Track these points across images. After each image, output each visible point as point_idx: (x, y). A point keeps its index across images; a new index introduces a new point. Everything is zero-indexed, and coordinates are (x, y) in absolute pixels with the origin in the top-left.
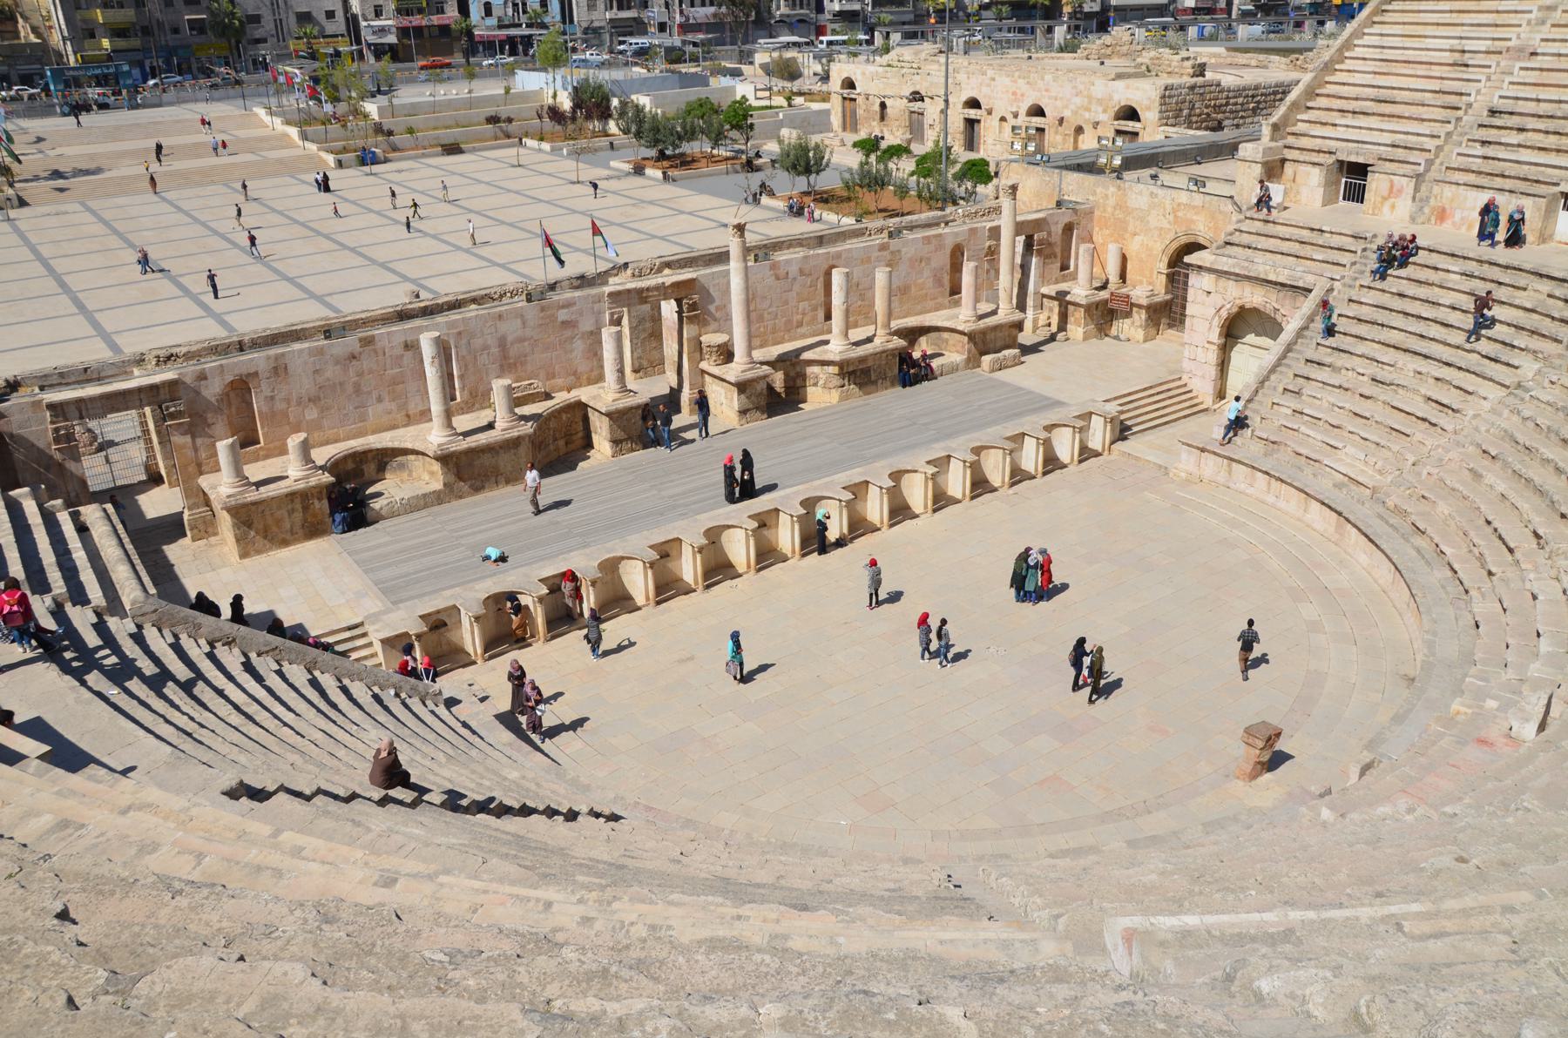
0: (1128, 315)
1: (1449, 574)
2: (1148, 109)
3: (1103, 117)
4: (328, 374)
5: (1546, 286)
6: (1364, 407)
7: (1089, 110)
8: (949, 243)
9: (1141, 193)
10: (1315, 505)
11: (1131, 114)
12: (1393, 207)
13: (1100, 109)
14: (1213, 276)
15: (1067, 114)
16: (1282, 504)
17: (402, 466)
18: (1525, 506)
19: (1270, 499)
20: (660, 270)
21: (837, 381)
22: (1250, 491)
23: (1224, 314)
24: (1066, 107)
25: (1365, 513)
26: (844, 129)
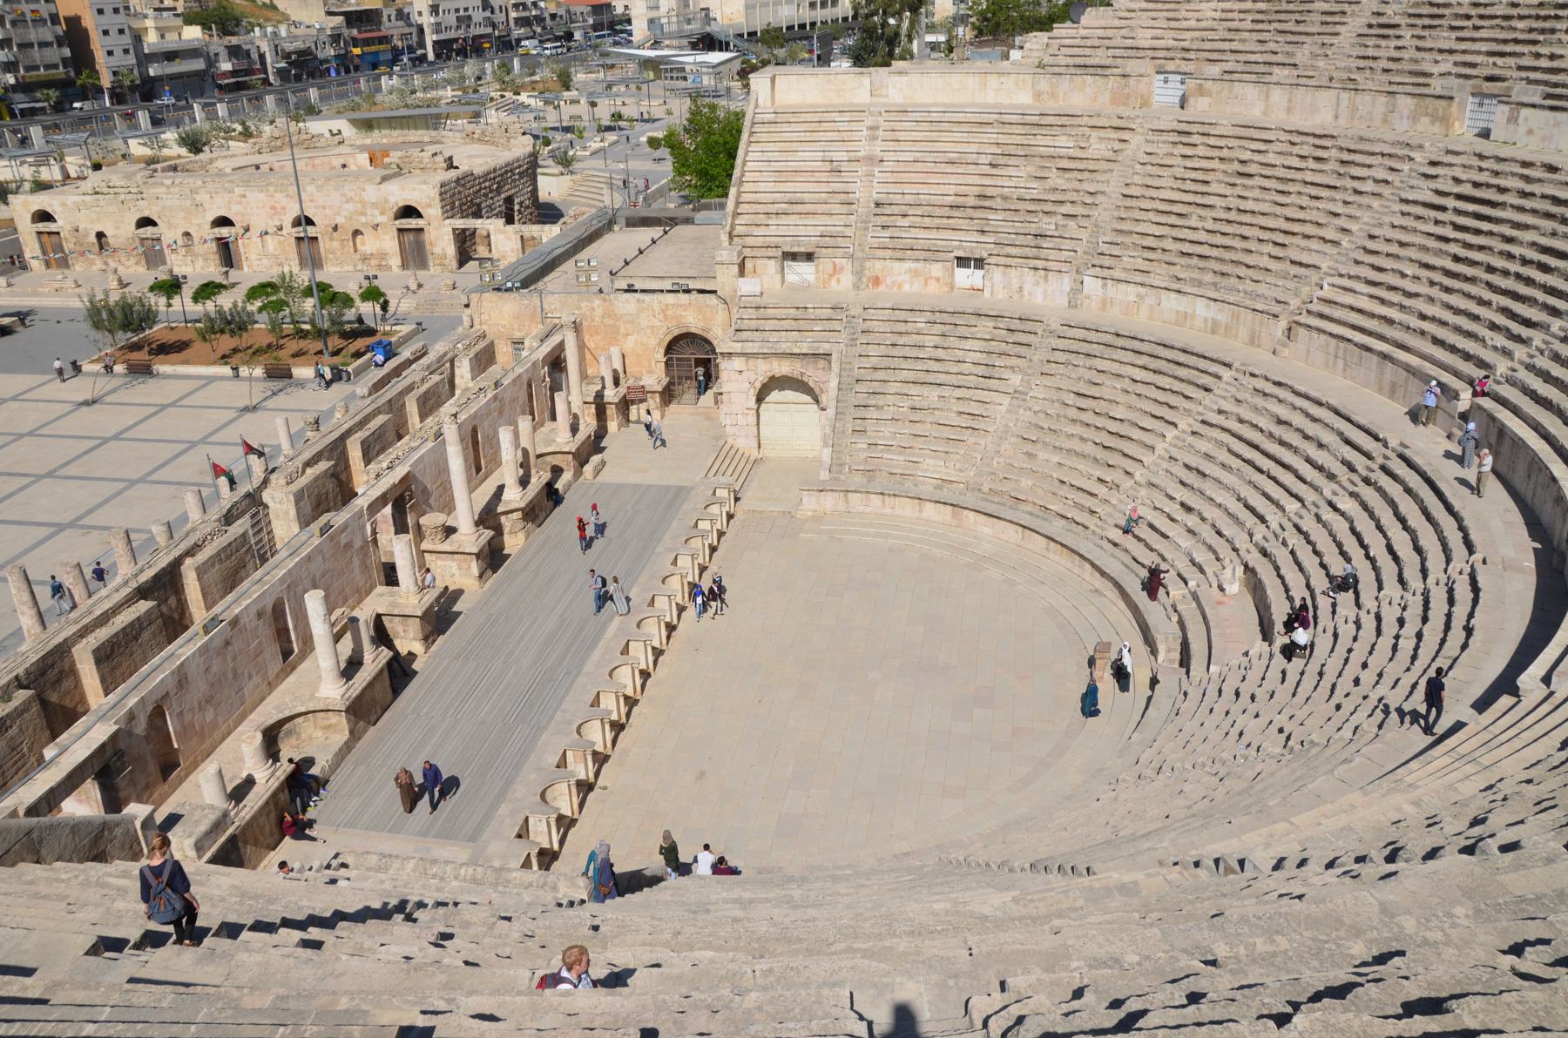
1: (1064, 522)
2: (429, 206)
3: (380, 219)
4: (214, 669)
5: (990, 323)
6: (918, 429)
10: (929, 506)
11: (409, 212)
13: (377, 212)
15: (340, 220)
16: (898, 512)
17: (289, 733)
18: (1081, 467)
19: (888, 511)
20: (303, 472)
21: (521, 524)
22: (868, 510)
23: (758, 385)
25: (969, 500)
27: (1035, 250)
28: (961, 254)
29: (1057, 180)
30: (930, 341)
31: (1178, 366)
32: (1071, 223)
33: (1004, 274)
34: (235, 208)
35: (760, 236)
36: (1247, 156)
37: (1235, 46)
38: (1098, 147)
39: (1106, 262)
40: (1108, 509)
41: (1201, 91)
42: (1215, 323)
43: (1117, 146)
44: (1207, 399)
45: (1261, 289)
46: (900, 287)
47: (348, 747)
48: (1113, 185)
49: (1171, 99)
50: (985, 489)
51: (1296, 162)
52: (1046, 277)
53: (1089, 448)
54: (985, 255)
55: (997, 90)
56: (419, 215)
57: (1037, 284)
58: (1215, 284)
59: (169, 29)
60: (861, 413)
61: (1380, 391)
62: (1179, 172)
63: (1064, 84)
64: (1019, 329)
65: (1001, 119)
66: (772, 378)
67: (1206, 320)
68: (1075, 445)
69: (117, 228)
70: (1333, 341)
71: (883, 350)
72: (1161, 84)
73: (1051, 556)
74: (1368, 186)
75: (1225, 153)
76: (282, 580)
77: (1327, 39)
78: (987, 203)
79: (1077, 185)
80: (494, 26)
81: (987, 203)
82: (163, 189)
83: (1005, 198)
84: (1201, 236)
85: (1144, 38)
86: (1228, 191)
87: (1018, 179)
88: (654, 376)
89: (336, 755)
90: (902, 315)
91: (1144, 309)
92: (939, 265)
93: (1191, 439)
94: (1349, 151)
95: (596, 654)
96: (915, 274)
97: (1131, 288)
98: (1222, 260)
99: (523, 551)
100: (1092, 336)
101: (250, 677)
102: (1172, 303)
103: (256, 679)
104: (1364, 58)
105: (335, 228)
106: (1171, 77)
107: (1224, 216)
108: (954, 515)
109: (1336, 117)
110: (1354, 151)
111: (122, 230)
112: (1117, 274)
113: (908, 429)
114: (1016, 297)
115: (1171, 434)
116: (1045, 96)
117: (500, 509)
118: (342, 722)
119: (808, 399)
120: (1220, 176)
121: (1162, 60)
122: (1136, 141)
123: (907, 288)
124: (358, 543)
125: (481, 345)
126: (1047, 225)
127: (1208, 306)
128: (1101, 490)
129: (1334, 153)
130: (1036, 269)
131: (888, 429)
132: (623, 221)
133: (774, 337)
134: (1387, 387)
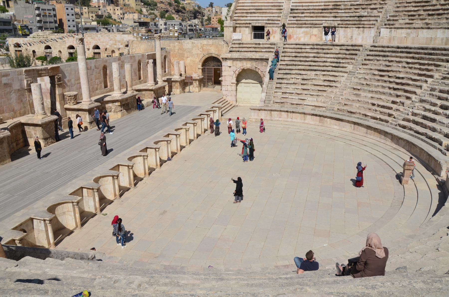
0: (191, 84)
3: (121, 46)
5: (338, 48)
6: (305, 87)
7: (116, 45)
9: (188, 43)
10: (309, 117)
12: (274, 37)
13: (120, 44)
14: (231, 61)
15: (108, 47)
19: (289, 120)
21: (120, 108)
23: (237, 73)
24: (107, 44)
27: (359, 22)
33: (345, 31)
35: (243, 20)
39: (391, 22)
40: (398, 113)
46: (299, 39)
52: (363, 31)
54: (336, 25)
59: (88, 22)
64: (352, 50)
66: (243, 70)
69: (39, 49)
73: (369, 136)
78: (338, 7)
80: (182, 30)
83: (345, 5)
88: (197, 74)
91: (410, 39)
92: (317, 29)
96: (306, 33)
97: (404, 31)
102: (424, 34)
112: (397, 26)
113: (301, 87)
115: (430, 80)
124: (16, 86)
128: (394, 106)
130: (359, 28)
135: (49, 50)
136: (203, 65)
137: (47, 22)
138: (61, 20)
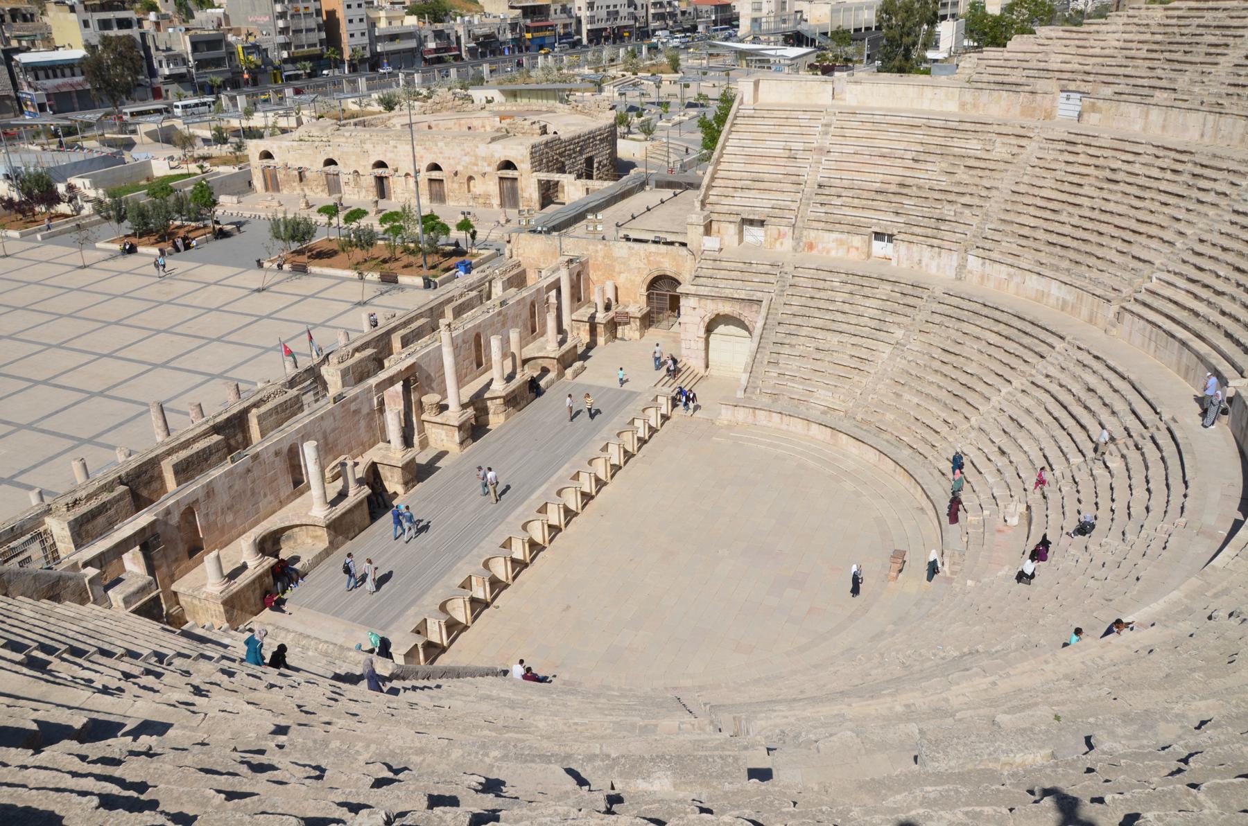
1: (911, 451)
2: (522, 162)
3: (487, 169)
4: (236, 487)
5: (888, 287)
6: (818, 365)
8: (528, 301)
10: (814, 427)
11: (508, 165)
15: (459, 168)
17: (289, 538)
18: (933, 409)
19: (784, 427)
20: (353, 355)
22: (770, 424)
23: (707, 320)
25: (846, 425)
26: (267, 189)
27: (934, 231)
28: (878, 230)
29: (962, 175)
30: (840, 297)
31: (1025, 333)
32: (967, 211)
33: (908, 248)
34: (389, 155)
35: (726, 205)
36: (1118, 165)
37: (1128, 71)
38: (1000, 150)
39: (988, 245)
40: (945, 445)
41: (1093, 108)
42: (1064, 301)
43: (1015, 150)
44: (1040, 364)
45: (1104, 278)
46: (828, 252)
47: (327, 553)
48: (1005, 183)
49: (1071, 114)
50: (859, 418)
51: (1156, 173)
53: (943, 395)
54: (895, 232)
55: (931, 100)
56: (515, 169)
57: (932, 258)
58: (1068, 270)
60: (778, 348)
61: (1178, 372)
62: (1060, 175)
63: (985, 97)
65: (927, 124)
66: (718, 315)
67: (1058, 299)
68: (933, 391)
70: (1149, 326)
71: (803, 301)
72: (1064, 100)
74: (1210, 198)
75: (1101, 162)
76: (298, 431)
77: (1207, 68)
78: (904, 191)
79: (977, 180)
80: (636, 19)
81: (904, 191)
82: (343, 140)
83: (919, 188)
84: (1067, 229)
85: (1055, 62)
86: (1096, 193)
87: (933, 173)
89: (316, 557)
90: (822, 275)
91: (1012, 285)
93: (1020, 395)
94: (1202, 166)
95: (520, 509)
96: (841, 243)
97: (1003, 267)
98: (1079, 251)
99: (501, 428)
100: (965, 304)
101: (265, 496)
103: (270, 498)
104: (1235, 85)
105: (456, 174)
106: (1072, 95)
107: (1087, 213)
108: (832, 436)
109: (1202, 136)
110: (1206, 166)
111: (315, 165)
112: (995, 255)
113: (811, 365)
114: (916, 267)
115: (1006, 389)
116: (969, 106)
117: (486, 396)
118: (324, 534)
119: (746, 334)
120: (1092, 181)
121: (1067, 80)
122: (1032, 148)
123: (833, 253)
124: (365, 411)
125: (515, 271)
126: (948, 211)
127: (1059, 288)
128: (944, 430)
129: (1189, 167)
131: (795, 363)
132: (653, 183)
133: (722, 284)
134: (1183, 369)
135: (333, 167)
136: (648, 289)
137: (301, 31)
138: (331, 14)
